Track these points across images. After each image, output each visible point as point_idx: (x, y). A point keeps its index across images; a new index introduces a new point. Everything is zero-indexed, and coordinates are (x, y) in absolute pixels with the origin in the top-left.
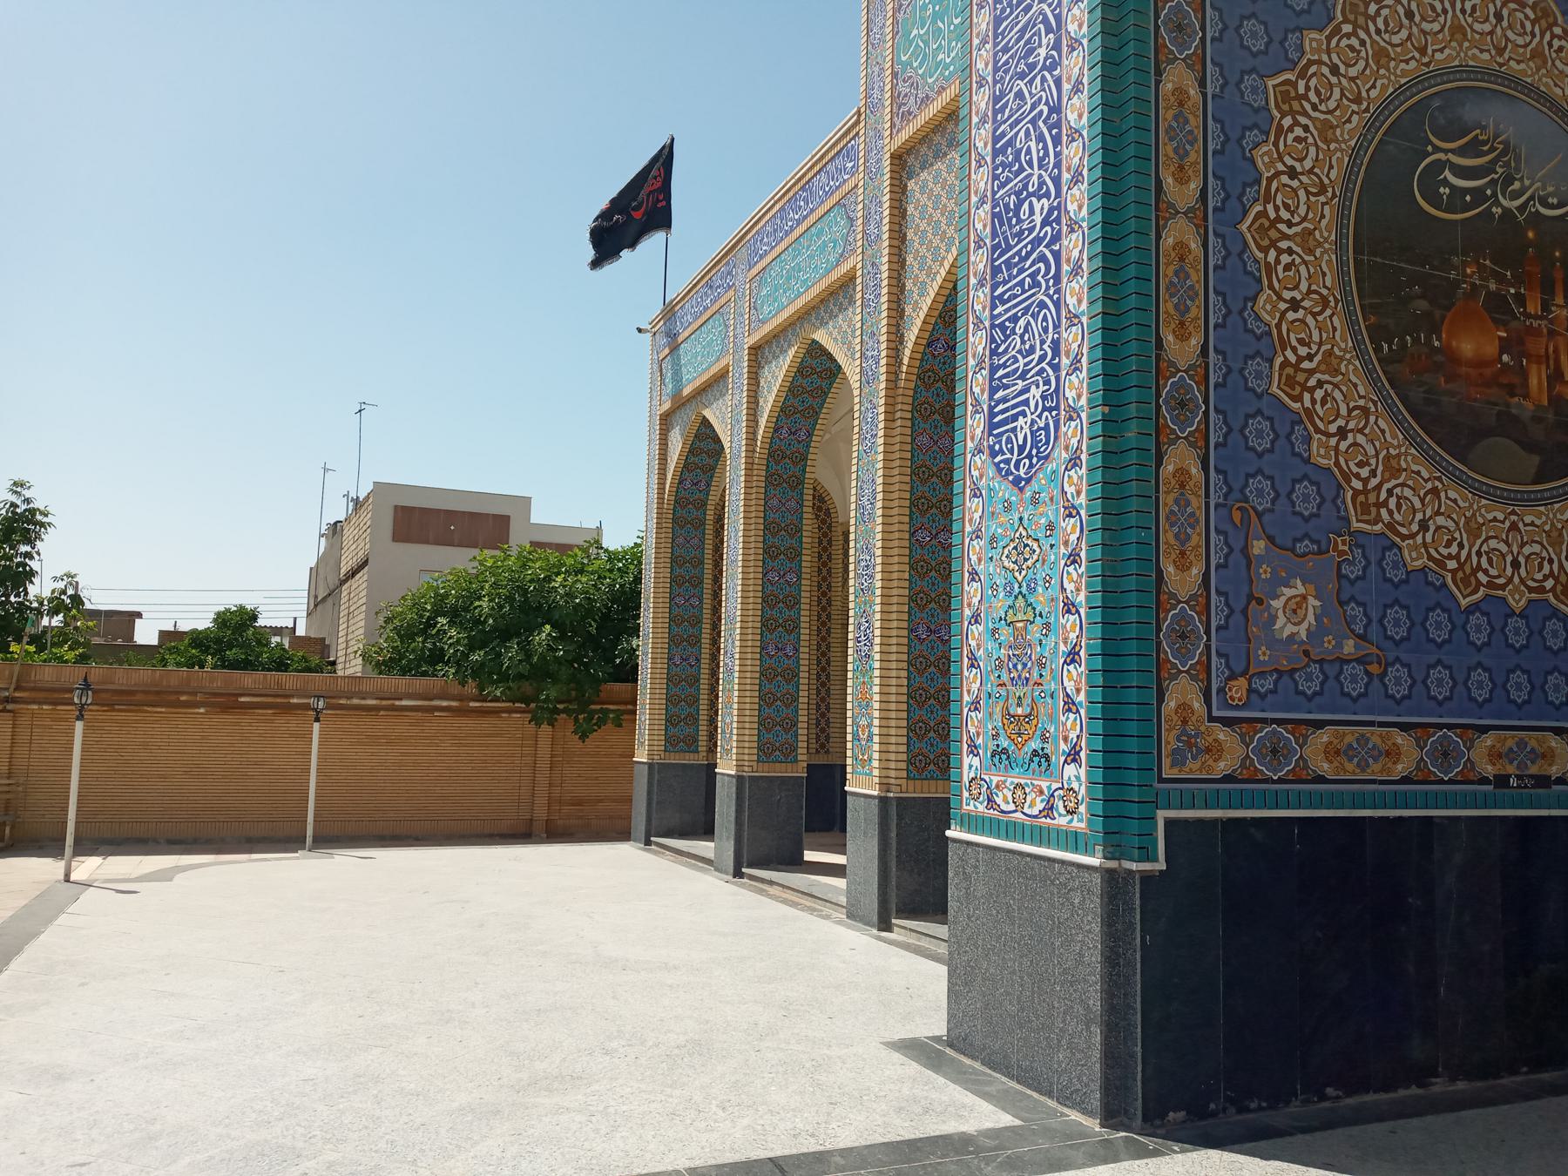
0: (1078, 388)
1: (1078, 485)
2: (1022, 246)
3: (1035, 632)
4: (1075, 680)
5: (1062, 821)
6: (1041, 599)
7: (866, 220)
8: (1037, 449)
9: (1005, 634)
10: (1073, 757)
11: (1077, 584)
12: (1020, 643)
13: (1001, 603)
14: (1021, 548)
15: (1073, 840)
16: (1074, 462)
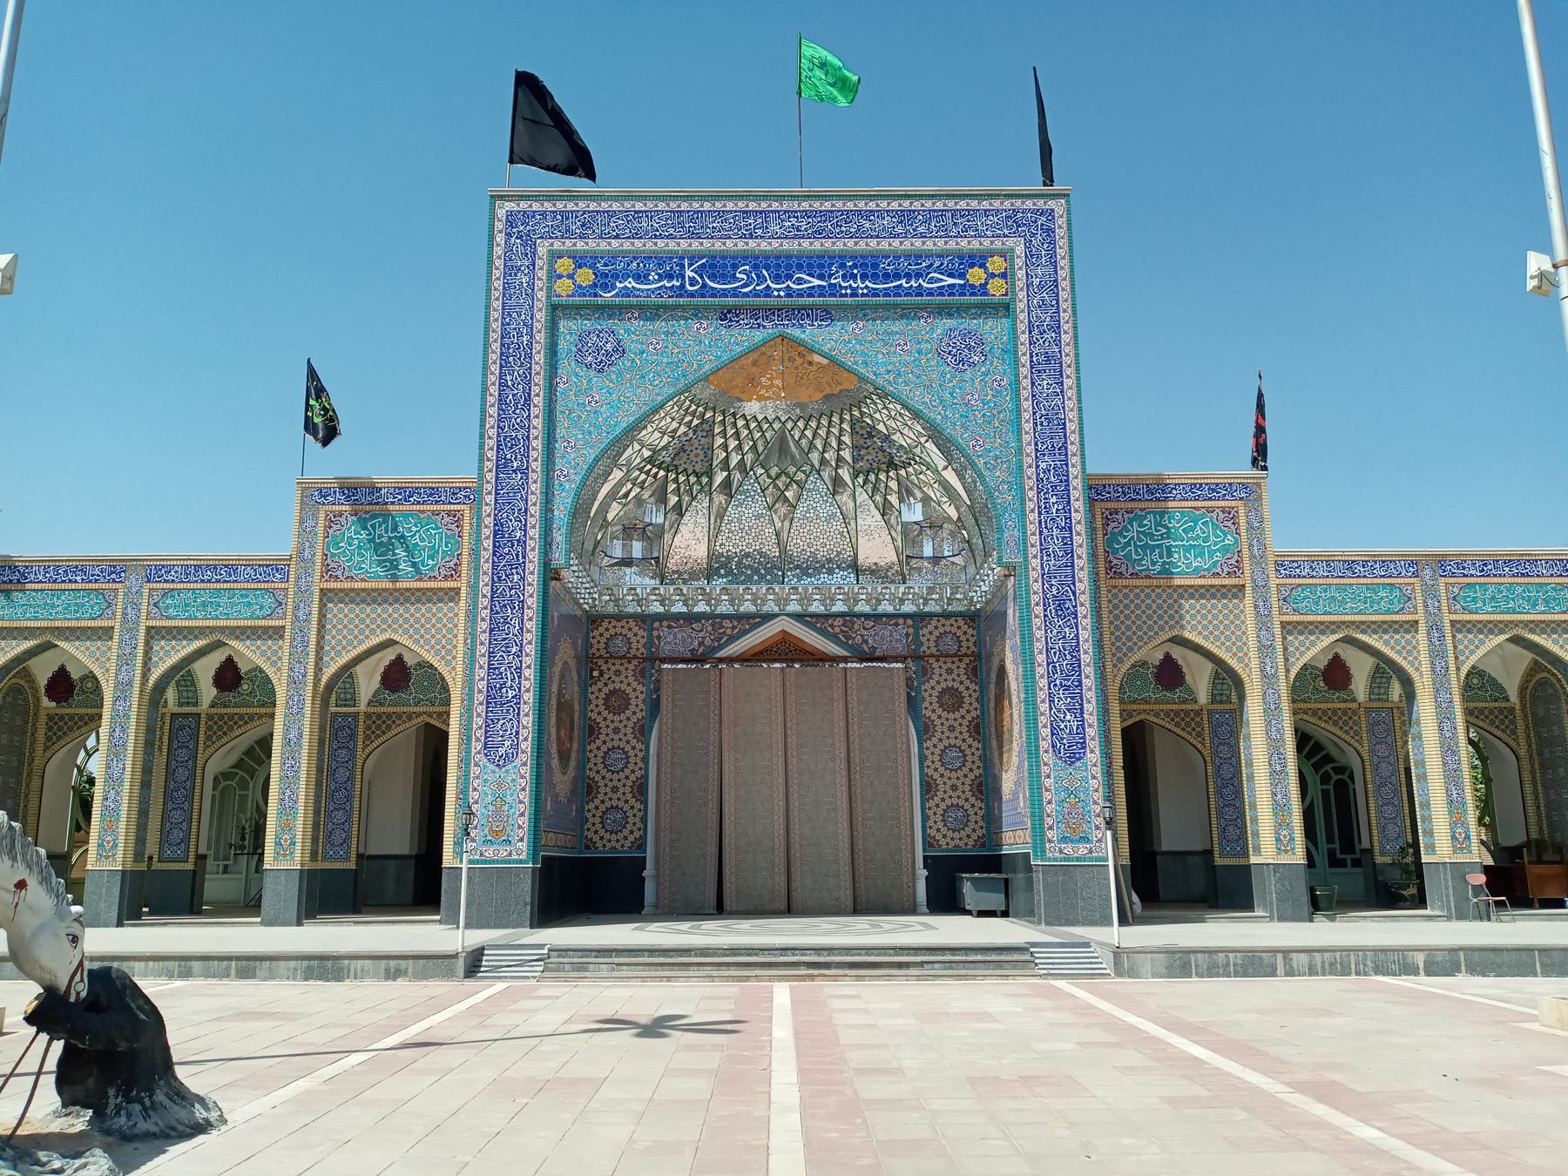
0: (527, 746)
1: (527, 771)
2: (504, 700)
3: (506, 808)
4: (524, 822)
5: (515, 857)
6: (509, 799)
7: (296, 608)
8: (508, 759)
9: (491, 808)
10: (521, 840)
11: (526, 797)
12: (498, 811)
13: (490, 798)
14: (500, 785)
15: (521, 861)
16: (525, 764)
